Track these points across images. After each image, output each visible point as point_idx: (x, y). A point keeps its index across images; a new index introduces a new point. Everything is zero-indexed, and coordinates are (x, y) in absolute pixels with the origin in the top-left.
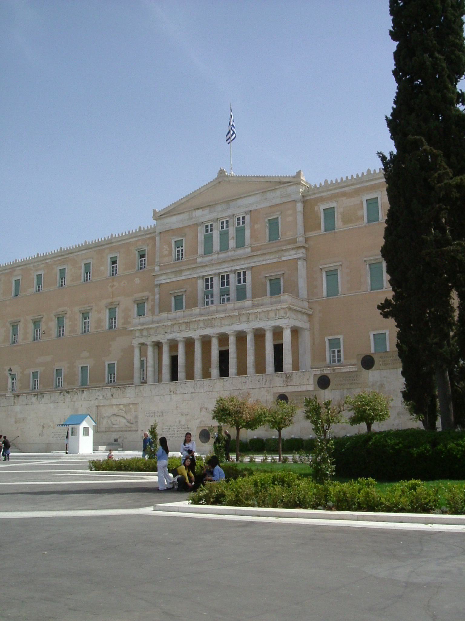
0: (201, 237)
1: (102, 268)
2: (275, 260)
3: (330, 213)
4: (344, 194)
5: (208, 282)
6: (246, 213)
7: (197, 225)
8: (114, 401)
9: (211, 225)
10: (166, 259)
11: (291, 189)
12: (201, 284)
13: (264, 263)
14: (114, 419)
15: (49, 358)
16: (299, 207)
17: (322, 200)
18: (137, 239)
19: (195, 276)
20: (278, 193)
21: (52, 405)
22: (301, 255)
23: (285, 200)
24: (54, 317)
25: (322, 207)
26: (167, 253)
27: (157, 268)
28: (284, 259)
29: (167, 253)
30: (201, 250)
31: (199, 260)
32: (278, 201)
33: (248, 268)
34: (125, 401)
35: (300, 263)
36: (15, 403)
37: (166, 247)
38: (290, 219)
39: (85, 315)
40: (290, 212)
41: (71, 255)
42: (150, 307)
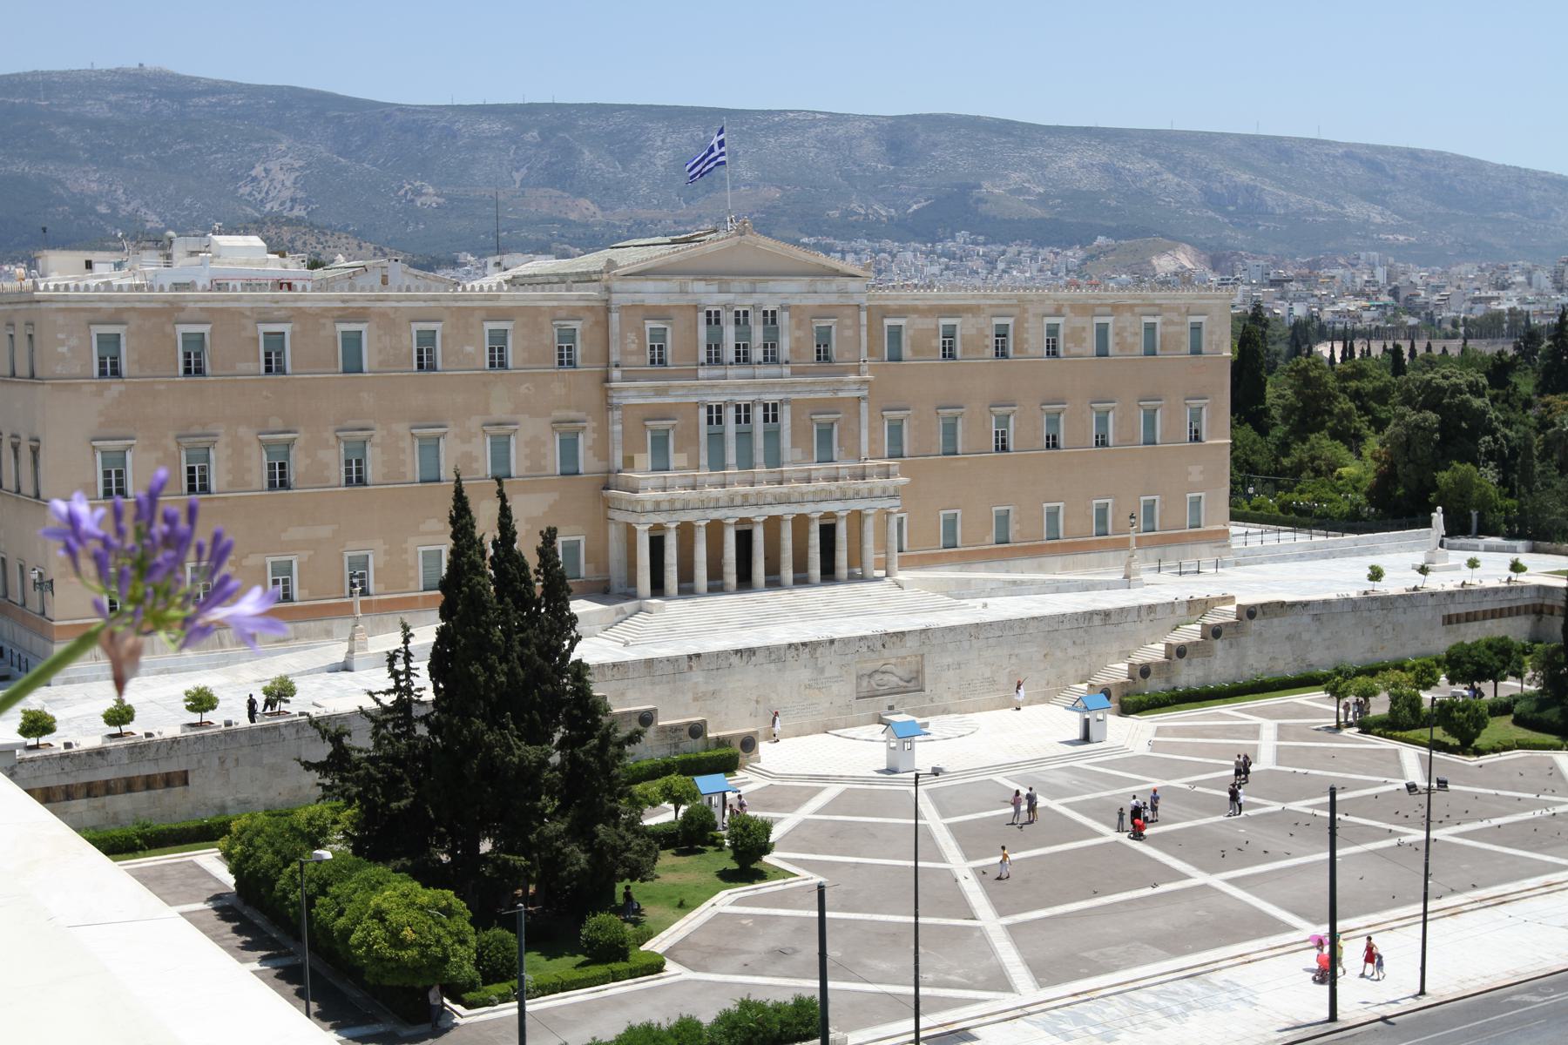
0: (702, 330)
1: (469, 349)
2: (828, 395)
3: (895, 333)
4: (916, 310)
5: (715, 415)
6: (784, 308)
7: (696, 308)
8: (886, 652)
9: (717, 313)
10: (633, 359)
11: (853, 285)
12: (703, 413)
13: (812, 396)
14: (877, 677)
15: (324, 531)
16: (864, 315)
17: (885, 312)
18: (555, 304)
19: (694, 399)
20: (834, 287)
21: (772, 666)
22: (865, 393)
23: (843, 301)
24: (333, 441)
25: (887, 322)
26: (634, 347)
27: (616, 373)
28: (841, 395)
29: (634, 347)
30: (703, 357)
31: (702, 372)
32: (833, 299)
33: (788, 401)
34: (903, 652)
35: (864, 405)
36: (691, 667)
37: (632, 336)
38: (849, 333)
39: (430, 448)
40: (848, 322)
41: (379, 304)
42: (590, 443)
